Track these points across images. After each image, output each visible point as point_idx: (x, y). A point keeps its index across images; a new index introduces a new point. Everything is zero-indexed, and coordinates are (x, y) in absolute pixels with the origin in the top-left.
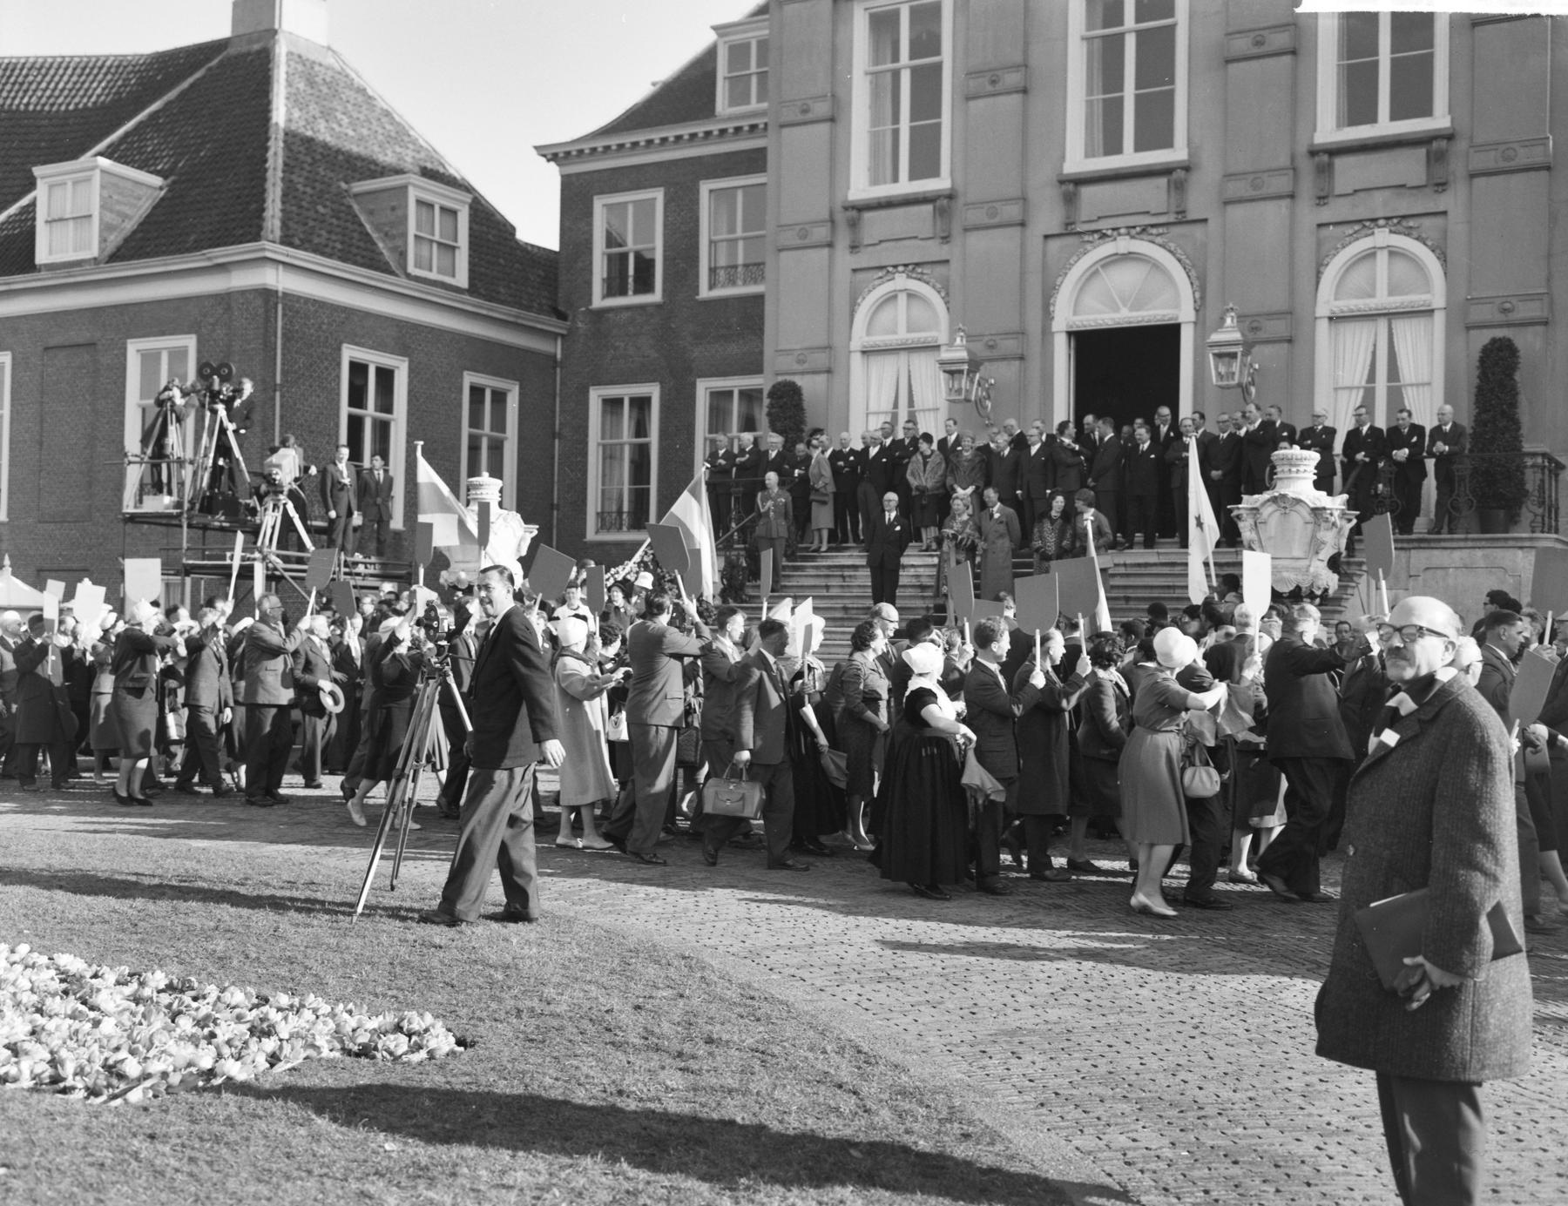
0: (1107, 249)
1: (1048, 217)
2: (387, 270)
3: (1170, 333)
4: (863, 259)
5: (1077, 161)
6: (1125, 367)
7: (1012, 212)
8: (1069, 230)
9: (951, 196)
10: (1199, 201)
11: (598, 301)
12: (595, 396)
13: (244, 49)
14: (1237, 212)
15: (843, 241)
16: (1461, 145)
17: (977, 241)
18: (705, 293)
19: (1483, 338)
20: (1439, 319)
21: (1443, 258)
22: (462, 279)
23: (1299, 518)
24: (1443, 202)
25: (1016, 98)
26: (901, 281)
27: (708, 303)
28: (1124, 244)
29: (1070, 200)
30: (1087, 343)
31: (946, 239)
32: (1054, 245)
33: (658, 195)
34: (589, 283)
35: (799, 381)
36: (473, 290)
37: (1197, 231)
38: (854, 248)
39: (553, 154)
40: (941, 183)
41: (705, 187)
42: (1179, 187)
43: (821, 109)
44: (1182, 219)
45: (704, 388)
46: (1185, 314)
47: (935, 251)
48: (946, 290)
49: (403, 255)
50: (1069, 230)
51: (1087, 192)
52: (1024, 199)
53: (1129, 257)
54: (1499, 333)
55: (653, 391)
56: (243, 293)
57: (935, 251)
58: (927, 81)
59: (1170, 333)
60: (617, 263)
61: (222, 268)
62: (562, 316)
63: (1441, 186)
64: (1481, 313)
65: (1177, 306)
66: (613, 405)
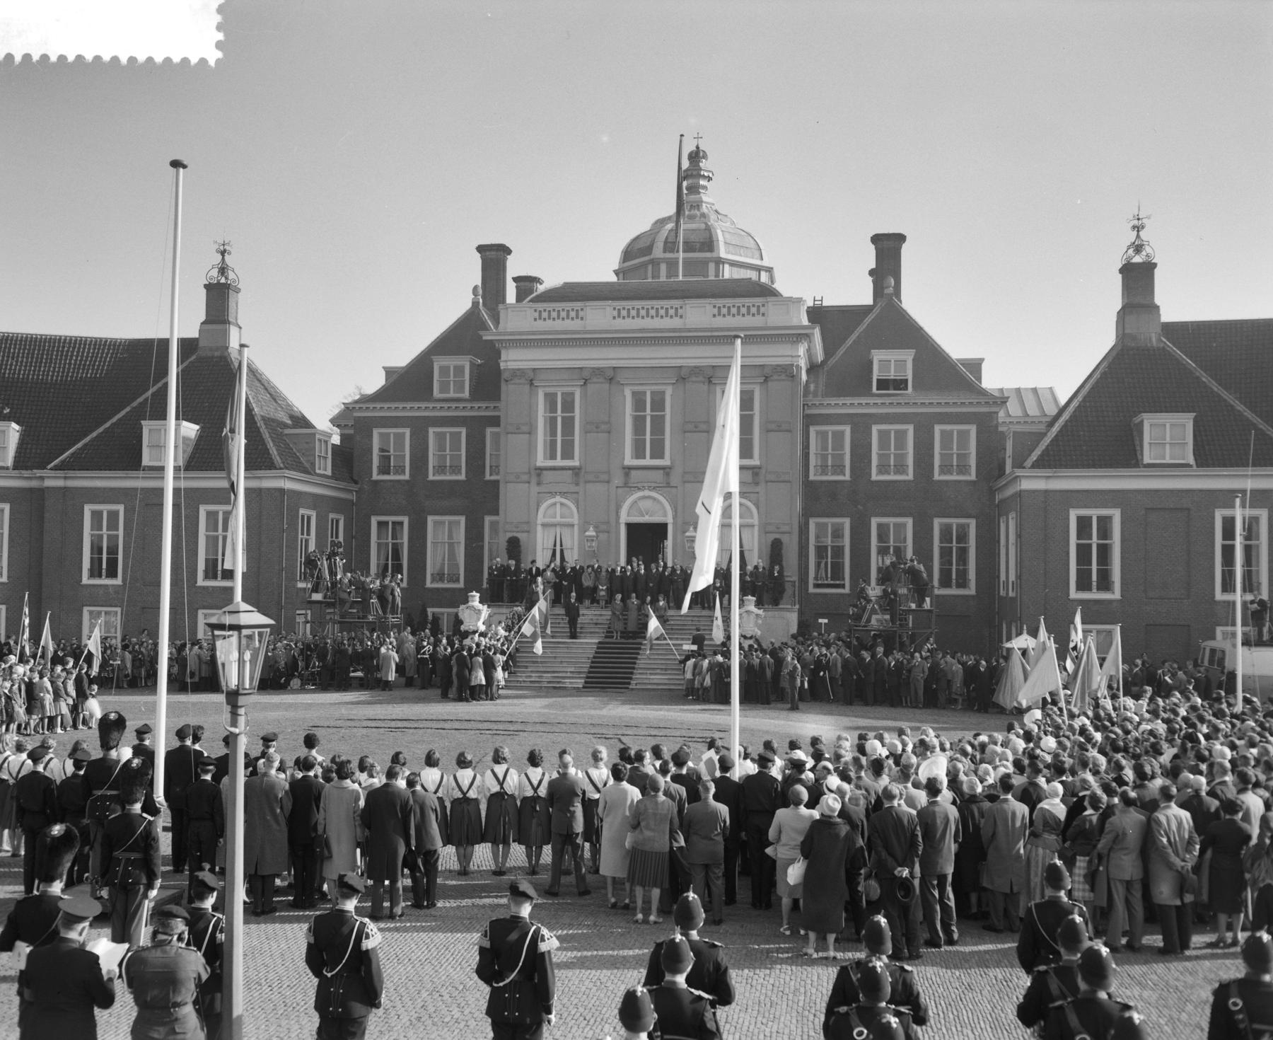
0: (640, 494)
1: (618, 480)
2: (308, 473)
3: (665, 526)
4: (543, 489)
5: (629, 461)
6: (647, 539)
7: (604, 477)
8: (626, 485)
9: (580, 468)
10: (675, 479)
11: (375, 477)
12: (374, 520)
13: (209, 354)
14: (687, 485)
15: (534, 480)
16: (763, 471)
17: (589, 486)
18: (431, 477)
19: (772, 537)
20: (756, 528)
21: (758, 508)
22: (329, 472)
23: (752, 617)
24: (757, 489)
25: (606, 435)
26: (558, 499)
27: (432, 482)
28: (647, 493)
29: (627, 475)
30: (631, 527)
31: (577, 484)
32: (620, 490)
33: (407, 431)
34: (371, 468)
35: (521, 536)
36: (334, 477)
37: (674, 490)
38: (539, 484)
40: (575, 463)
41: (431, 430)
42: (668, 474)
43: (525, 428)
44: (668, 485)
45: (430, 519)
46: (669, 520)
47: (573, 488)
48: (577, 503)
49: (313, 464)
50: (626, 485)
51: (633, 473)
52: (608, 472)
53: (649, 497)
54: (777, 536)
55: (405, 520)
56: (269, 489)
57: (573, 488)
58: (568, 424)
59: (665, 526)
60: (385, 459)
61: (176, 447)
62: (356, 483)
63: (757, 484)
64: (770, 528)
65: (665, 515)
66: (380, 524)
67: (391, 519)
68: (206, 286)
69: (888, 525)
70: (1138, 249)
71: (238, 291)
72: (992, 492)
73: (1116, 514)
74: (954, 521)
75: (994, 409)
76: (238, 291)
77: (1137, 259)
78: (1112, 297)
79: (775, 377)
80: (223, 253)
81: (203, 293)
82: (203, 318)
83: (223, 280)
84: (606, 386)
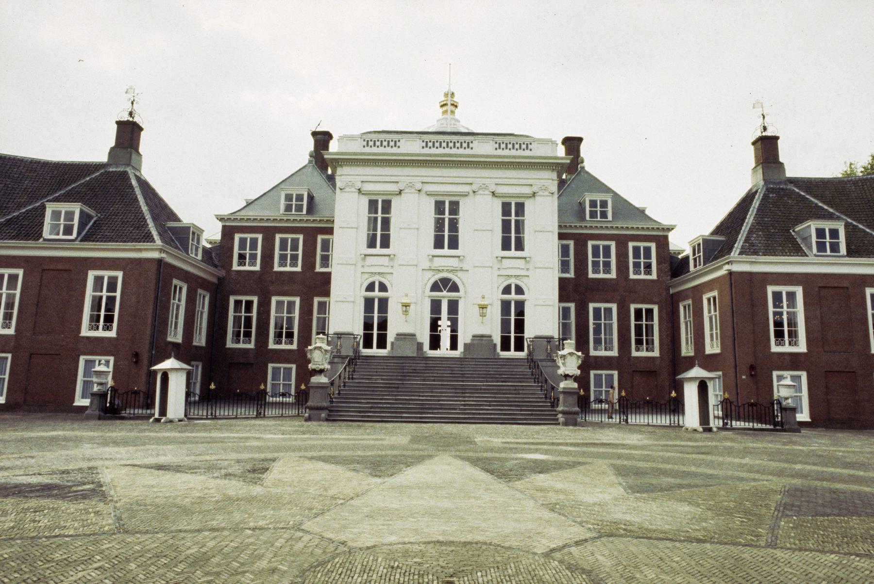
12: (232, 299)
39: (221, 219)
45: (274, 300)
55: (255, 299)
67: (244, 298)
68: (119, 123)
69: (600, 309)
70: (765, 129)
71: (141, 129)
72: (668, 289)
73: (799, 291)
74: (644, 307)
75: (665, 234)
76: (141, 129)
77: (764, 134)
78: (749, 156)
79: (540, 193)
80: (132, 103)
81: (116, 126)
82: (113, 144)
83: (131, 119)
84: (417, 195)
